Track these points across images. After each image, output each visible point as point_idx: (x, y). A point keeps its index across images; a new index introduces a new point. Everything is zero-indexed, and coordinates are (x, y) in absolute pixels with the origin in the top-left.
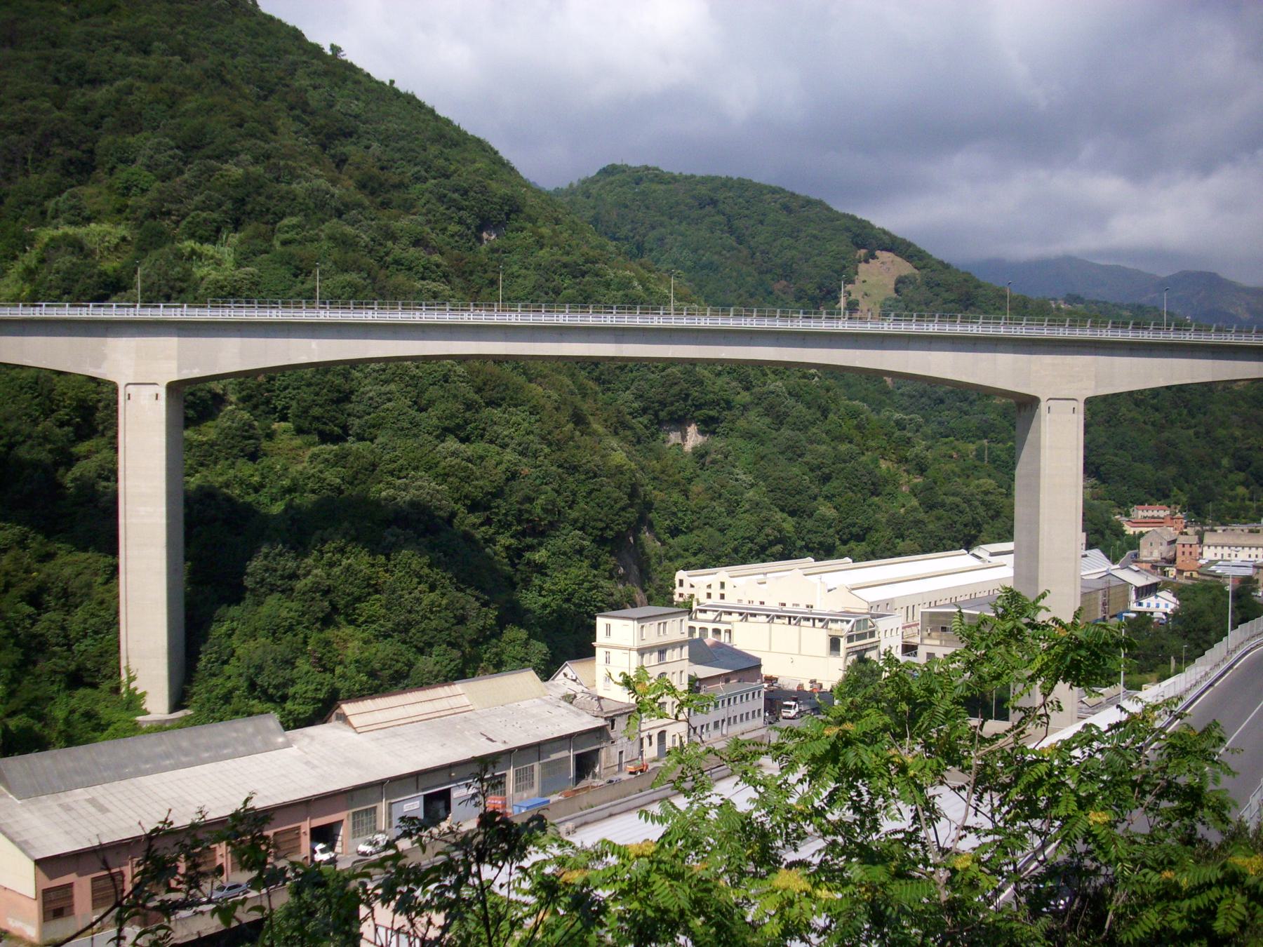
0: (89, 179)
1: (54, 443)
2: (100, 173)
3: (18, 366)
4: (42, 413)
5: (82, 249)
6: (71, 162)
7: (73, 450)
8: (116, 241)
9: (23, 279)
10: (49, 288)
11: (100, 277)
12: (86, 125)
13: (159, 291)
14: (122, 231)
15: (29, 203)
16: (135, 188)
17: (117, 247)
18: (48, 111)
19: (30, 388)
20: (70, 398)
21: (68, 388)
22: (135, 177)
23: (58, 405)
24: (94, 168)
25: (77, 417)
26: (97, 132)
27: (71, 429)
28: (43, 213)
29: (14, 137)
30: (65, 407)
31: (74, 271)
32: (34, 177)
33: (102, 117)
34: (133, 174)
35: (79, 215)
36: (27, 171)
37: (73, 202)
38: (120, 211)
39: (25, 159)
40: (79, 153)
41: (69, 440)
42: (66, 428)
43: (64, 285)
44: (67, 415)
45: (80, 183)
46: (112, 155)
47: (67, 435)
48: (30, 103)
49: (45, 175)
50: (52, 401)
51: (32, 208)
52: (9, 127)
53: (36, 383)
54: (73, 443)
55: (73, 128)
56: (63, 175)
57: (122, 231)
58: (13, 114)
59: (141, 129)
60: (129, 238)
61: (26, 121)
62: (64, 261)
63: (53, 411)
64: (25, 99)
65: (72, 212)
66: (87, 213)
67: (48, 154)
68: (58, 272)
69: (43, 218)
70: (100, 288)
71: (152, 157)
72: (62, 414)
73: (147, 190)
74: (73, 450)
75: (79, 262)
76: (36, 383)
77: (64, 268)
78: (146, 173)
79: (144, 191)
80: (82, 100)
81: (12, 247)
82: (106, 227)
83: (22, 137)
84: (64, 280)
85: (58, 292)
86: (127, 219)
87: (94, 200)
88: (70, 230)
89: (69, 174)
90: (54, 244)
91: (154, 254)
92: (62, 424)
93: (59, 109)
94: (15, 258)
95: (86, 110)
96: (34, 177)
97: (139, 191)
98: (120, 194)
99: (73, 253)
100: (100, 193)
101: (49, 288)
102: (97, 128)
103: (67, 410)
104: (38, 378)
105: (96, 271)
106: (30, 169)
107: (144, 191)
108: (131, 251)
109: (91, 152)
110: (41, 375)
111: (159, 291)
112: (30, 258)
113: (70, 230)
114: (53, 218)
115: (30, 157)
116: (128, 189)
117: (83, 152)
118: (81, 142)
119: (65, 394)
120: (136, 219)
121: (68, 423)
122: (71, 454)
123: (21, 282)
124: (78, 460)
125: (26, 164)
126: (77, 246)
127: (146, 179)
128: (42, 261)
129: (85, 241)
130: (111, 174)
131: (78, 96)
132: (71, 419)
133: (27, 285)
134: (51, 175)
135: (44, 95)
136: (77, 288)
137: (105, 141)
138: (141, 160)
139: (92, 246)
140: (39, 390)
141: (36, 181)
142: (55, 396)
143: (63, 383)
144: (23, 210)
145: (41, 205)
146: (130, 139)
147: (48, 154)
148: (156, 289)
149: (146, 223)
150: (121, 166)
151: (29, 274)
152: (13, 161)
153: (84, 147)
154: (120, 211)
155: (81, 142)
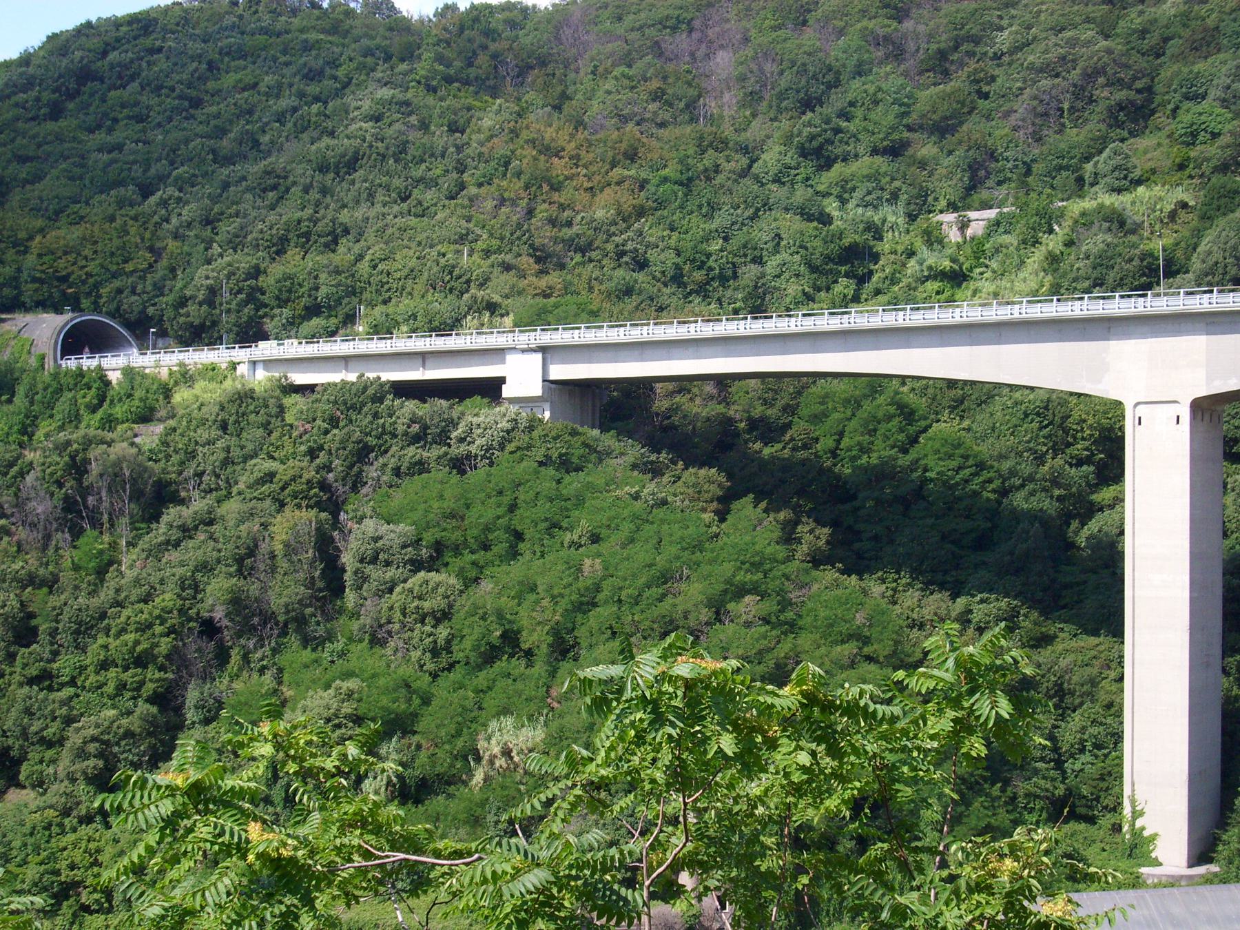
0: (1146, 127)
1: (1068, 487)
2: (1160, 118)
3: (1027, 387)
4: (1053, 448)
5: (1122, 223)
6: (1121, 107)
7: (1093, 497)
8: (1169, 208)
9: (1044, 270)
10: (1075, 280)
11: (1142, 260)
12: (1143, 54)
13: (1225, 274)
14: (1181, 194)
15: (1060, 168)
16: (1202, 133)
17: (1173, 216)
18: (1088, 43)
19: (1038, 414)
20: (1091, 427)
21: (1088, 414)
22: (1203, 118)
23: (1075, 438)
24: (1153, 112)
25: (1101, 452)
26: (1159, 61)
27: (1092, 468)
28: (1080, 181)
29: (1045, 83)
30: (1083, 439)
31: (1109, 254)
32: (1072, 133)
33: (1166, 40)
34: (1200, 114)
35: (1125, 178)
36: (1063, 125)
37: (1118, 160)
38: (1181, 167)
39: (1061, 110)
40: (1132, 95)
41: (1088, 484)
42: (1085, 468)
43: (1096, 274)
44: (1086, 449)
45: (1133, 134)
46: (1175, 91)
47: (1086, 477)
48: (1068, 34)
49: (1087, 127)
50: (1066, 431)
51: (1064, 174)
52: (1041, 70)
53: (1046, 408)
54: (1095, 488)
55: (1124, 60)
56: (1110, 126)
57: (1181, 194)
58: (1046, 52)
59: (1219, 50)
60: (1192, 203)
61: (1063, 58)
62: (1096, 241)
63: (1069, 445)
64: (1063, 29)
65: (1116, 174)
66: (1137, 174)
67: (1091, 101)
68: (1088, 257)
69: (1080, 186)
70: (1144, 275)
71: (1228, 87)
72: (1079, 449)
73: (1219, 134)
74: (1093, 497)
75: (1115, 241)
76: (1046, 408)
77: (1095, 250)
78: (1219, 110)
79: (1215, 136)
80: (1139, 20)
81: (1033, 229)
82: (1158, 190)
83: (1057, 81)
84: (1095, 268)
85: (1086, 284)
86: (1191, 177)
87: (1149, 156)
88: (1108, 200)
89: (1120, 125)
90: (1085, 221)
91: (1221, 222)
92: (1080, 463)
93: (1107, 37)
94: (1036, 242)
95: (1143, 33)
96: (1072, 133)
97: (1208, 136)
98: (1183, 143)
99: (1110, 230)
100: (1159, 145)
101: (1075, 280)
102: (1158, 56)
103: (1087, 443)
104: (1049, 401)
105: (1137, 252)
106: (1067, 123)
107: (1215, 136)
108: (1193, 218)
109: (1149, 89)
110: (1054, 397)
111: (1225, 274)
112: (1053, 243)
113: (1108, 200)
114: (1092, 185)
115: (1066, 106)
116: (1194, 135)
117: (1139, 91)
118: (1135, 78)
119: (1084, 421)
120: (1202, 176)
121: (1087, 461)
122: (1092, 504)
123: (1042, 274)
124: (1101, 509)
125: (1062, 116)
126: (1117, 221)
127: (1219, 119)
128: (1069, 244)
129: (1128, 213)
130: (1174, 118)
131: (1133, 16)
132: (1093, 455)
133: (1049, 278)
134: (1094, 126)
135: (1088, 20)
136: (1112, 276)
137: (1169, 71)
138: (1214, 93)
139: (1137, 219)
140: (1051, 417)
141: (1076, 136)
142: (1071, 423)
143: (1081, 406)
144: (1054, 178)
145: (1078, 169)
146: (1199, 66)
147: (1091, 101)
148: (1221, 270)
149: (1214, 180)
150: (1186, 105)
151: (1053, 260)
152: (1046, 114)
153: (1139, 84)
154: (1181, 167)
155: (1135, 78)
